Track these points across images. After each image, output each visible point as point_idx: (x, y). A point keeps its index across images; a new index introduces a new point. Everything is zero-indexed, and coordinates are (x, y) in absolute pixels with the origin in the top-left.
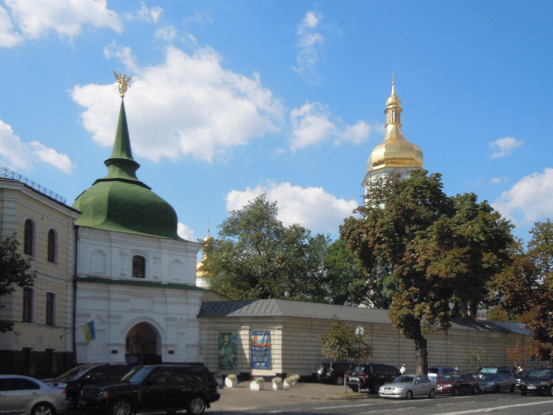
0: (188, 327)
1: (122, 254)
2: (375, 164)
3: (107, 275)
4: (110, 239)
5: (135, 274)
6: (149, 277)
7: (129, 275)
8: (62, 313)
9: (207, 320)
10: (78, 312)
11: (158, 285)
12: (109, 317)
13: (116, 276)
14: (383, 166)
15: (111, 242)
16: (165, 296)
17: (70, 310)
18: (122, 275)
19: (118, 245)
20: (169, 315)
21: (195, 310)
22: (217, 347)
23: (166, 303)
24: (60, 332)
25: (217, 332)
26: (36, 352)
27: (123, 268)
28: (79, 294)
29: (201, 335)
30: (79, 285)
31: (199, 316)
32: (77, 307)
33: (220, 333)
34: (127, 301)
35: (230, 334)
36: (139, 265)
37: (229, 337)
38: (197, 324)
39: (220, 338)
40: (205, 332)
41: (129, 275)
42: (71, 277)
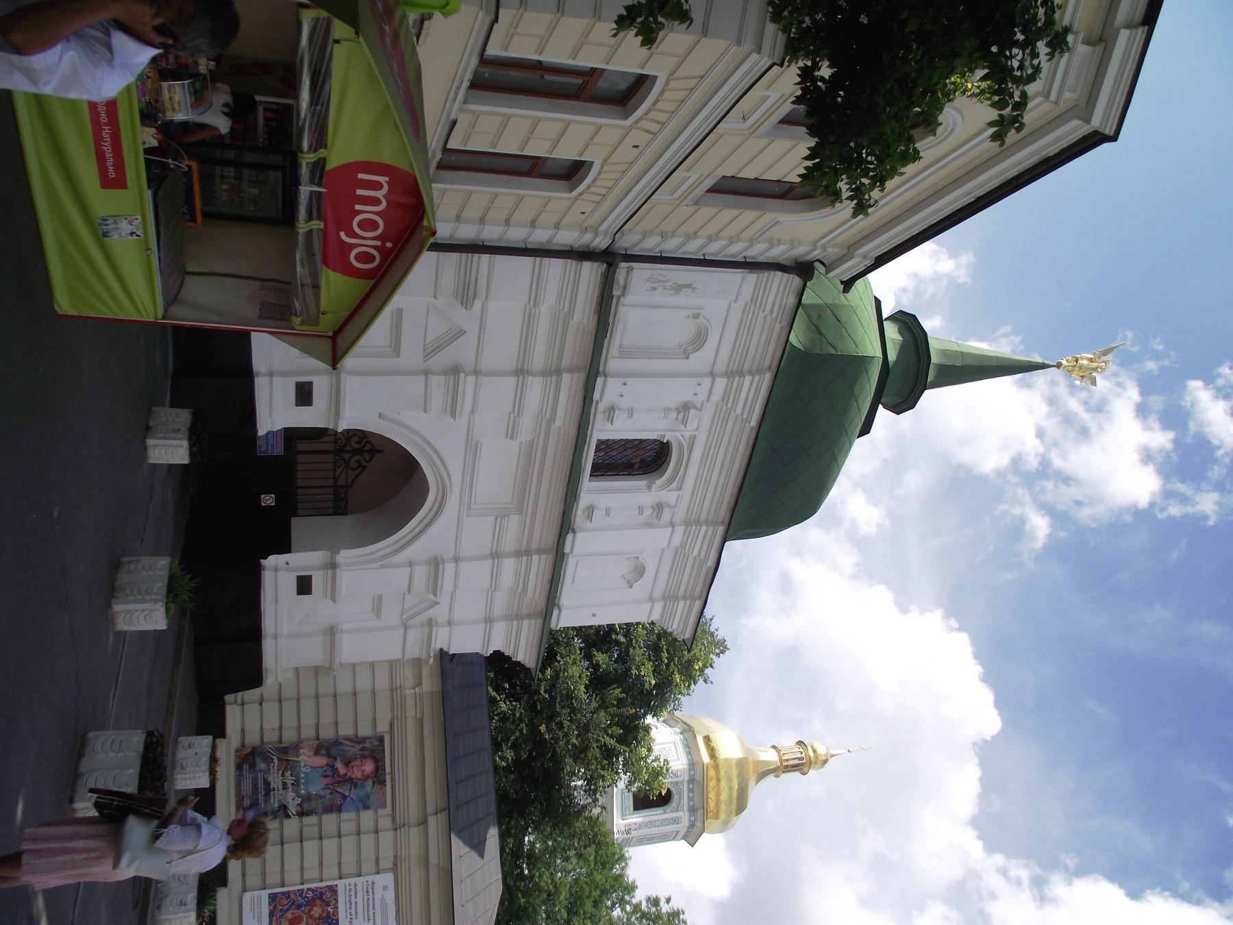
0: (406, 626)
1: (685, 408)
2: (707, 739)
3: (613, 362)
6: (593, 492)
9: (429, 684)
12: (455, 371)
13: (609, 391)
14: (706, 758)
15: (729, 374)
16: (522, 552)
17: (491, 234)
19: (717, 396)
20: (449, 568)
22: (327, 733)
23: (495, 555)
25: (383, 727)
27: (630, 414)
28: (555, 267)
29: (372, 665)
30: (590, 272)
31: (443, 655)
32: (500, 259)
33: (381, 739)
34: (512, 433)
35: (378, 777)
37: (365, 778)
38: (413, 652)
39: (364, 740)
40: (382, 683)
42: (627, 242)
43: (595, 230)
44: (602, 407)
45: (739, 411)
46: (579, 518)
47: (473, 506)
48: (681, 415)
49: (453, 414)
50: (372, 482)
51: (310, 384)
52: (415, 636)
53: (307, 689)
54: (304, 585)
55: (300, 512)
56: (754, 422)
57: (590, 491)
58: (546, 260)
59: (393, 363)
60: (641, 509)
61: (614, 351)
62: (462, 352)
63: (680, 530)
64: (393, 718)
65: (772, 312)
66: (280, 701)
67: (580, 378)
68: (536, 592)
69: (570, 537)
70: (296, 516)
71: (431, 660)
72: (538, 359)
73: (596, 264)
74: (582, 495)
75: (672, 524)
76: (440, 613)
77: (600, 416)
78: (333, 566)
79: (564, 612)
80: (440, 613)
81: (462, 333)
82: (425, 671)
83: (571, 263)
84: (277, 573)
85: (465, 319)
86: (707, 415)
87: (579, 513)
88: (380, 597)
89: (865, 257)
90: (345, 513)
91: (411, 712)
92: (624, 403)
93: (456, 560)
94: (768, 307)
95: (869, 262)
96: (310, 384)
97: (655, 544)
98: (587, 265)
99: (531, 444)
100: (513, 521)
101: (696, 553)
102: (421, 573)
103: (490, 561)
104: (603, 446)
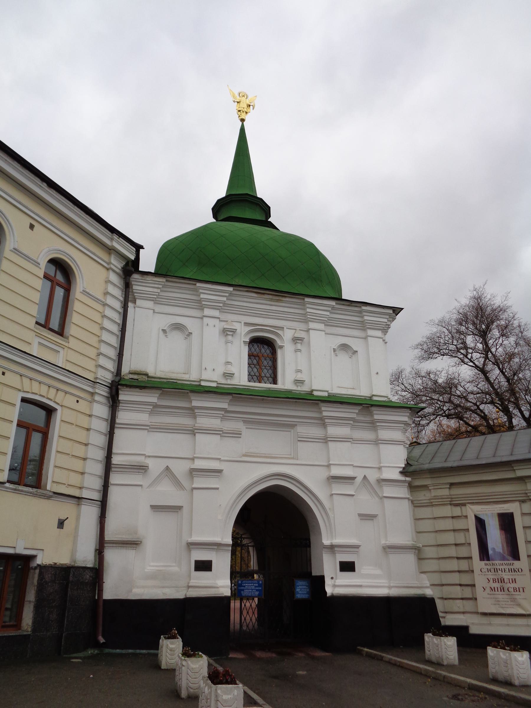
1: (225, 332)
3: (193, 376)
4: (200, 301)
6: (286, 382)
7: (241, 378)
10: (116, 460)
11: (307, 400)
18: (228, 375)
19: (216, 313)
20: (336, 471)
21: (395, 458)
28: (122, 417)
30: (124, 396)
31: (404, 472)
34: (237, 434)
38: (403, 492)
41: (241, 378)
43: (92, 394)
44: (223, 381)
45: (225, 299)
46: (305, 388)
47: (292, 456)
48: (228, 333)
49: (220, 471)
50: (275, 524)
51: (197, 562)
52: (388, 491)
53: (433, 565)
55: (309, 571)
56: (231, 289)
57: (284, 384)
58: (118, 421)
59: (185, 510)
60: (297, 351)
61: (186, 377)
62: (180, 468)
63: (312, 325)
64: (451, 504)
65: (158, 288)
66: (443, 585)
67: (193, 396)
68: (351, 413)
69: (315, 393)
70: (311, 573)
71: (408, 479)
72: (187, 421)
73: (120, 392)
74: (286, 388)
75: (308, 331)
76: (373, 476)
77: (229, 382)
78: (332, 548)
79: (374, 393)
80: (373, 476)
81: (167, 468)
82: (418, 483)
83: (121, 406)
84: (337, 584)
85: (155, 467)
86: (230, 317)
87: (299, 389)
88: (360, 515)
89: (112, 239)
90: (309, 540)
91: (445, 492)
92: (221, 370)
93: (329, 466)
94: (156, 290)
95: (115, 237)
96: (197, 562)
97: (321, 341)
98: (121, 397)
99: (244, 422)
100: (302, 430)
101: (328, 313)
102: (338, 488)
103: (330, 443)
104: (251, 377)
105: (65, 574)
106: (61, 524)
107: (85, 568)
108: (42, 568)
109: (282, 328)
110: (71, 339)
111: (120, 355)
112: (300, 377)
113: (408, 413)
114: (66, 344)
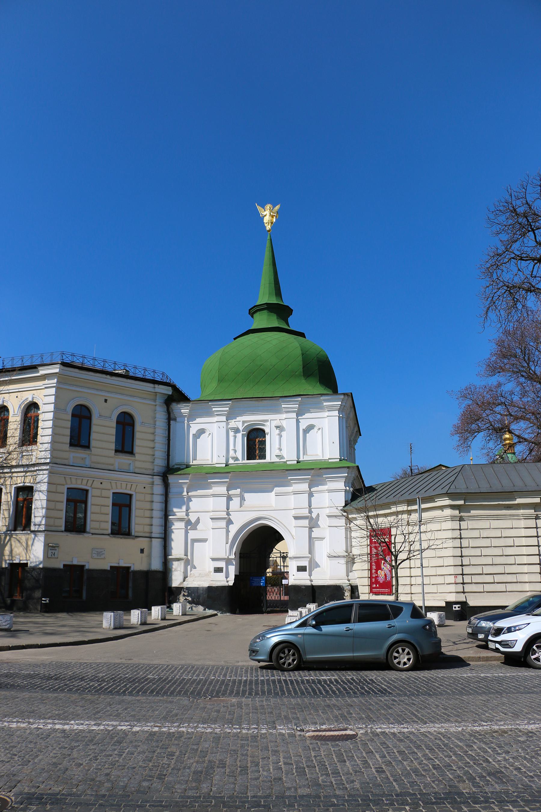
5: (251, 455)
8: (141, 518)
24: (143, 543)
26: (90, 571)
36: (255, 442)
38: (342, 522)
54: (301, 569)
95: (156, 386)
105: (147, 574)
106: (142, 551)
107: (156, 572)
108: (135, 572)
109: (266, 421)
110: (136, 455)
111: (168, 455)
112: (277, 452)
113: (346, 470)
114: (134, 458)
